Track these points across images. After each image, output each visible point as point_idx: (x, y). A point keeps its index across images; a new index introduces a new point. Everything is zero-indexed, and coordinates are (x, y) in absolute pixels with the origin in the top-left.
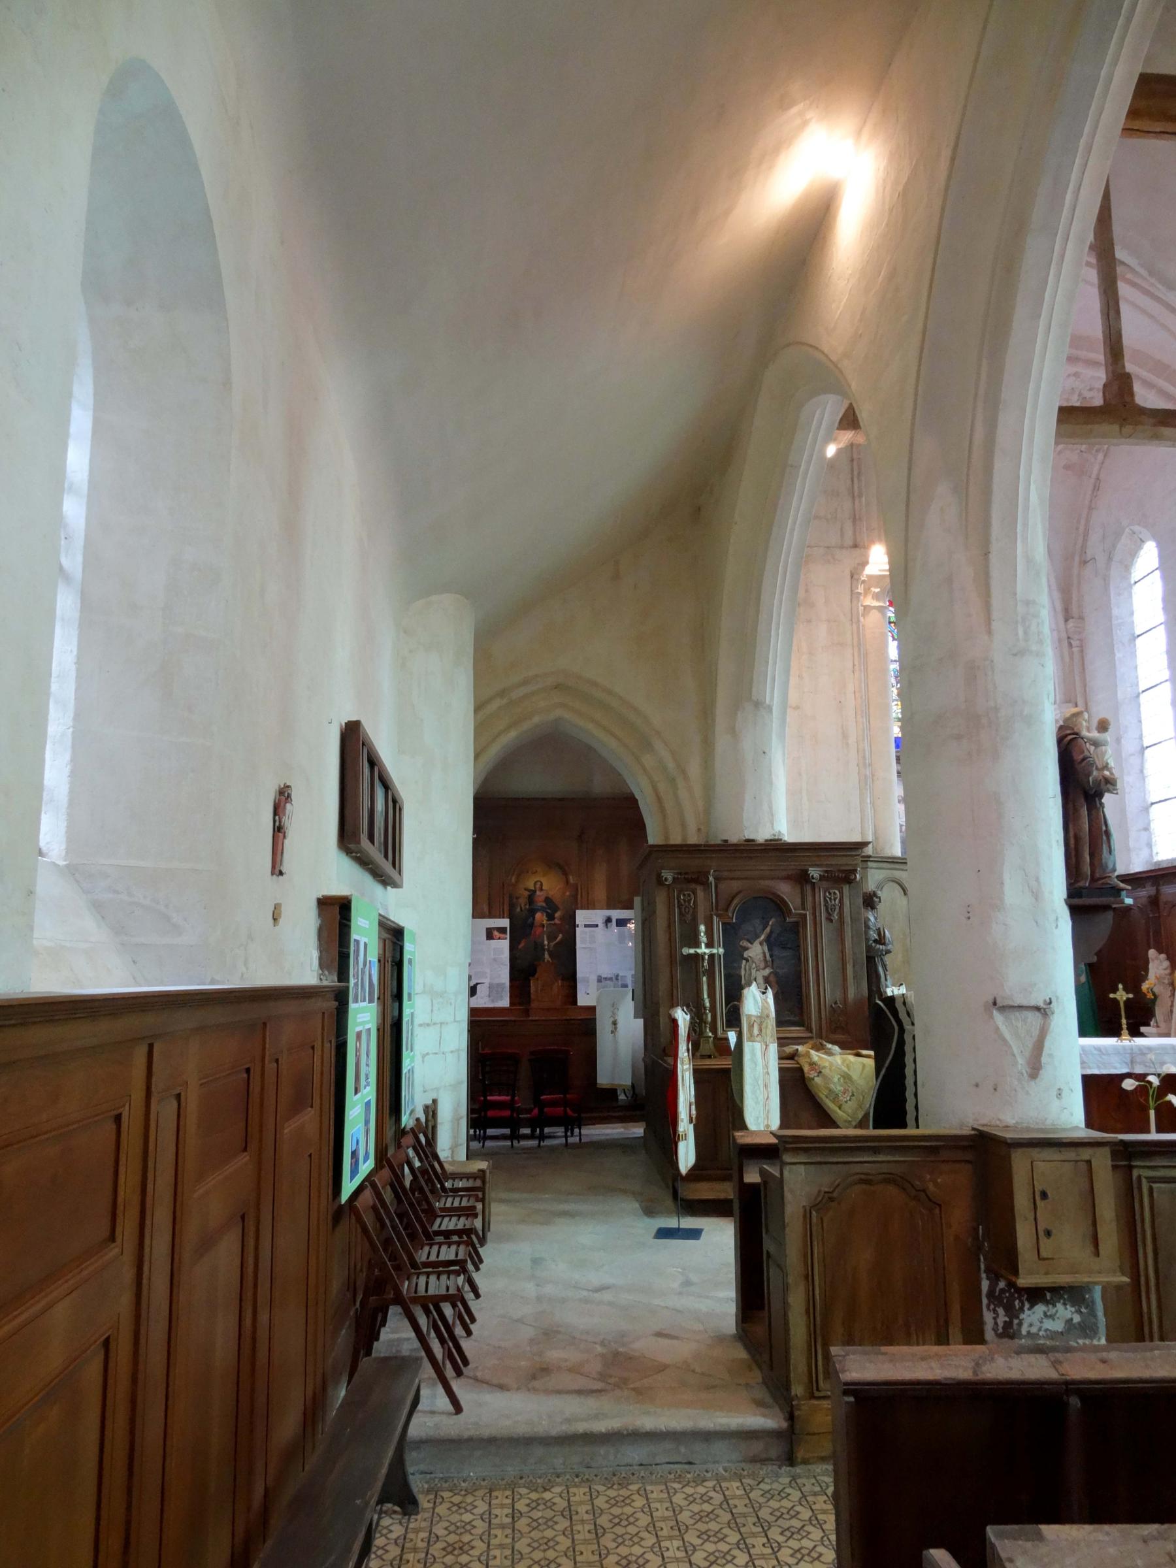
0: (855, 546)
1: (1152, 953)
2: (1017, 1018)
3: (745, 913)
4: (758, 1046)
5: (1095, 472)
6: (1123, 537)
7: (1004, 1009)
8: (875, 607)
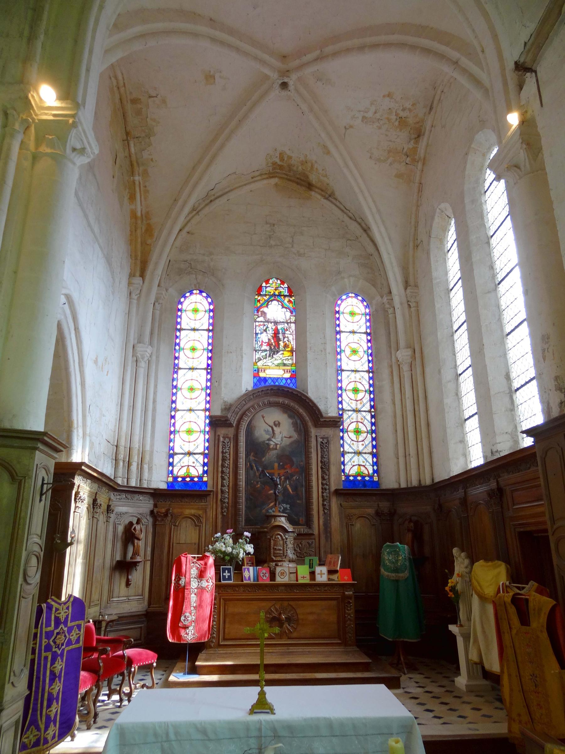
1: (455, 551)
5: (418, 178)
6: (436, 217)
8: (47, 154)
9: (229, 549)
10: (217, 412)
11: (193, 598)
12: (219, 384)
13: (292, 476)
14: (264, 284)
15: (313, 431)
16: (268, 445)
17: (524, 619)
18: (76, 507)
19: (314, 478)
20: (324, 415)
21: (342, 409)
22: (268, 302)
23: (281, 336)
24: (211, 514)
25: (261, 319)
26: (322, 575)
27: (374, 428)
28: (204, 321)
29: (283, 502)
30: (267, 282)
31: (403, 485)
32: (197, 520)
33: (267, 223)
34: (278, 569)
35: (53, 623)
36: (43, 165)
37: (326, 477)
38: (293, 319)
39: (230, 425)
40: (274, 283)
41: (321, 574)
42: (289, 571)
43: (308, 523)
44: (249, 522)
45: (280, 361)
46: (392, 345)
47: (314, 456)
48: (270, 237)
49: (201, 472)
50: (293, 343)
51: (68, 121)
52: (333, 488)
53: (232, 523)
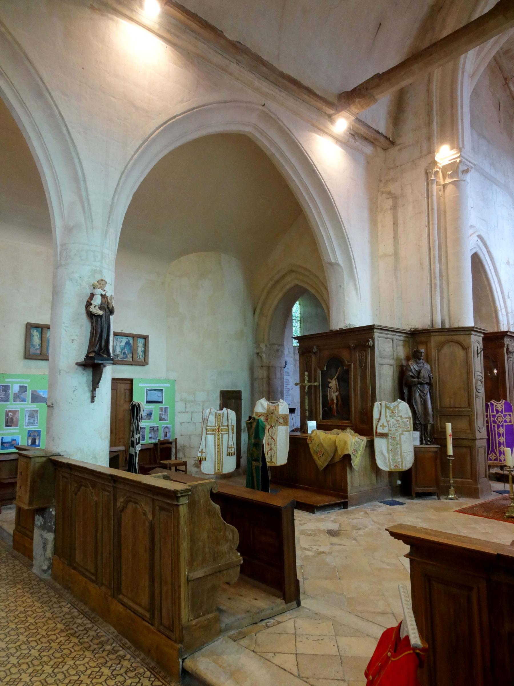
18: (508, 357)
35: (495, 412)
51: (456, 161)
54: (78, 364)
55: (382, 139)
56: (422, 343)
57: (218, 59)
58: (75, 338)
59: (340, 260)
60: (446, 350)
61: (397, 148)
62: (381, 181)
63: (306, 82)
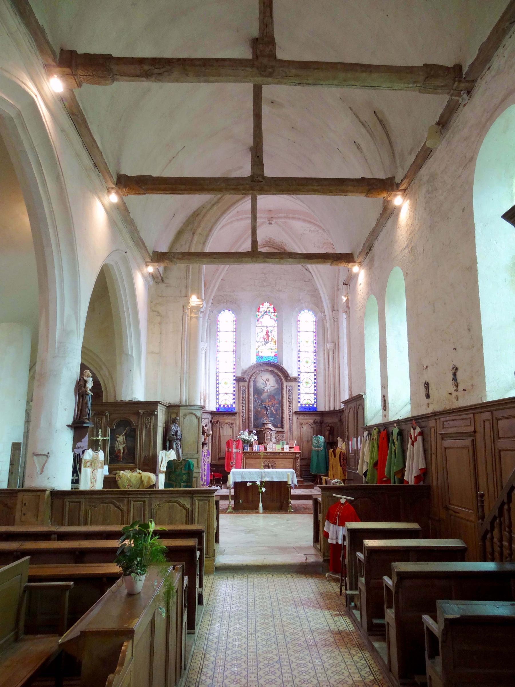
0: (186, 296)
1: (339, 439)
2: (40, 458)
3: (118, 425)
4: (89, 470)
7: (37, 455)
9: (247, 438)
10: (239, 375)
11: (234, 456)
12: (240, 360)
13: (275, 405)
14: (261, 306)
15: (285, 384)
16: (264, 390)
17: (335, 456)
19: (285, 406)
20: (290, 375)
21: (300, 372)
22: (263, 315)
23: (270, 334)
24: (237, 422)
25: (260, 325)
26: (287, 449)
27: (315, 381)
28: (232, 326)
29: (271, 417)
30: (263, 304)
31: (327, 410)
32: (231, 425)
33: (262, 273)
34: (268, 447)
36: (194, 320)
37: (291, 405)
38: (276, 325)
39: (245, 381)
40: (266, 305)
41: (286, 448)
42: (273, 447)
43: (282, 426)
44: (255, 426)
45: (270, 348)
46: (325, 340)
47: (285, 395)
48: (264, 281)
49: (232, 403)
50: (276, 338)
52: (294, 411)
53: (247, 426)
54: (67, 426)
55: (160, 278)
56: (173, 413)
57: (121, 225)
58: (66, 407)
59: (134, 354)
60: (188, 417)
61: (164, 285)
62: (152, 302)
63: (146, 244)
